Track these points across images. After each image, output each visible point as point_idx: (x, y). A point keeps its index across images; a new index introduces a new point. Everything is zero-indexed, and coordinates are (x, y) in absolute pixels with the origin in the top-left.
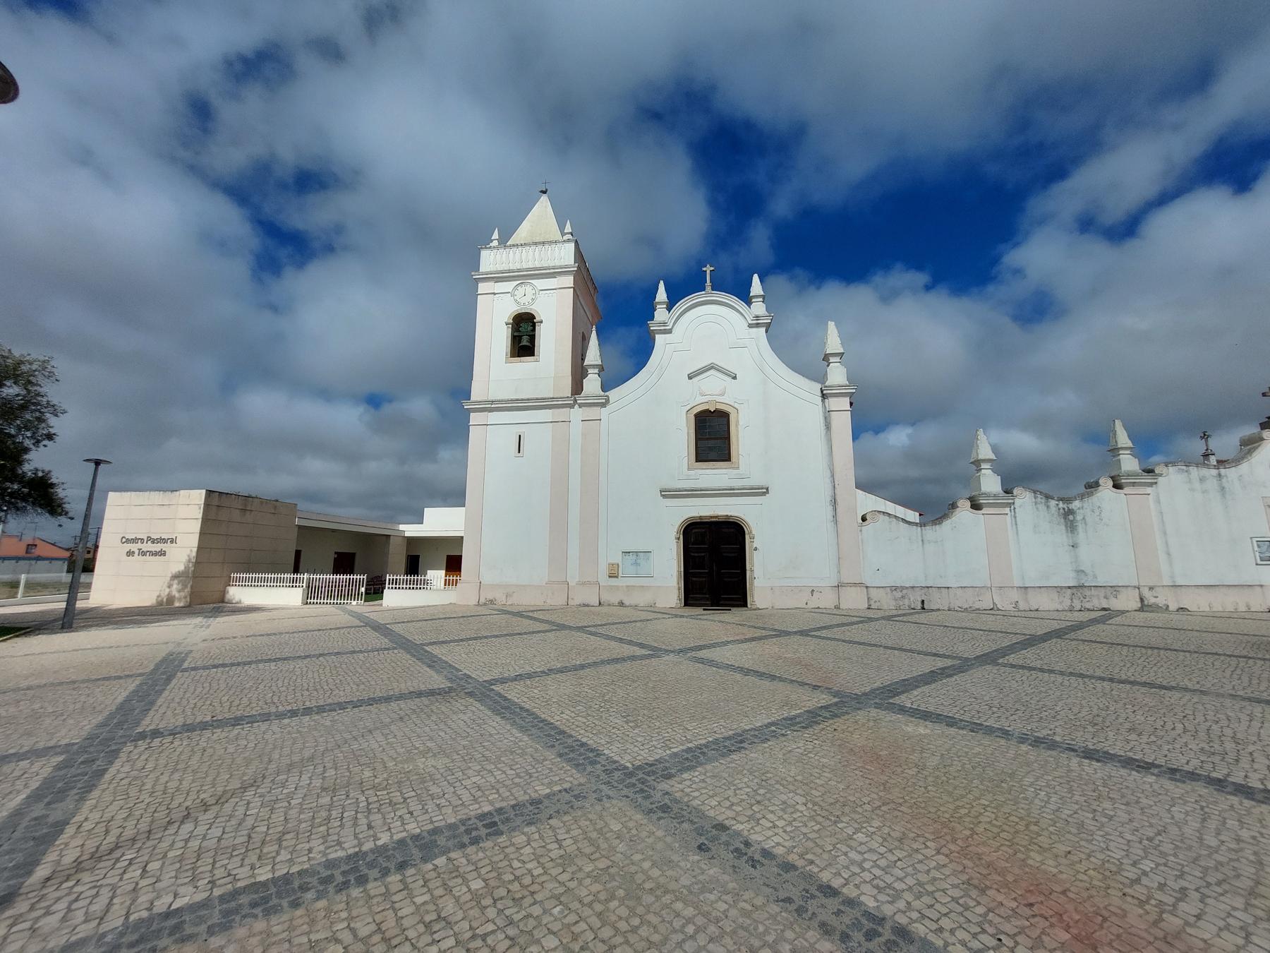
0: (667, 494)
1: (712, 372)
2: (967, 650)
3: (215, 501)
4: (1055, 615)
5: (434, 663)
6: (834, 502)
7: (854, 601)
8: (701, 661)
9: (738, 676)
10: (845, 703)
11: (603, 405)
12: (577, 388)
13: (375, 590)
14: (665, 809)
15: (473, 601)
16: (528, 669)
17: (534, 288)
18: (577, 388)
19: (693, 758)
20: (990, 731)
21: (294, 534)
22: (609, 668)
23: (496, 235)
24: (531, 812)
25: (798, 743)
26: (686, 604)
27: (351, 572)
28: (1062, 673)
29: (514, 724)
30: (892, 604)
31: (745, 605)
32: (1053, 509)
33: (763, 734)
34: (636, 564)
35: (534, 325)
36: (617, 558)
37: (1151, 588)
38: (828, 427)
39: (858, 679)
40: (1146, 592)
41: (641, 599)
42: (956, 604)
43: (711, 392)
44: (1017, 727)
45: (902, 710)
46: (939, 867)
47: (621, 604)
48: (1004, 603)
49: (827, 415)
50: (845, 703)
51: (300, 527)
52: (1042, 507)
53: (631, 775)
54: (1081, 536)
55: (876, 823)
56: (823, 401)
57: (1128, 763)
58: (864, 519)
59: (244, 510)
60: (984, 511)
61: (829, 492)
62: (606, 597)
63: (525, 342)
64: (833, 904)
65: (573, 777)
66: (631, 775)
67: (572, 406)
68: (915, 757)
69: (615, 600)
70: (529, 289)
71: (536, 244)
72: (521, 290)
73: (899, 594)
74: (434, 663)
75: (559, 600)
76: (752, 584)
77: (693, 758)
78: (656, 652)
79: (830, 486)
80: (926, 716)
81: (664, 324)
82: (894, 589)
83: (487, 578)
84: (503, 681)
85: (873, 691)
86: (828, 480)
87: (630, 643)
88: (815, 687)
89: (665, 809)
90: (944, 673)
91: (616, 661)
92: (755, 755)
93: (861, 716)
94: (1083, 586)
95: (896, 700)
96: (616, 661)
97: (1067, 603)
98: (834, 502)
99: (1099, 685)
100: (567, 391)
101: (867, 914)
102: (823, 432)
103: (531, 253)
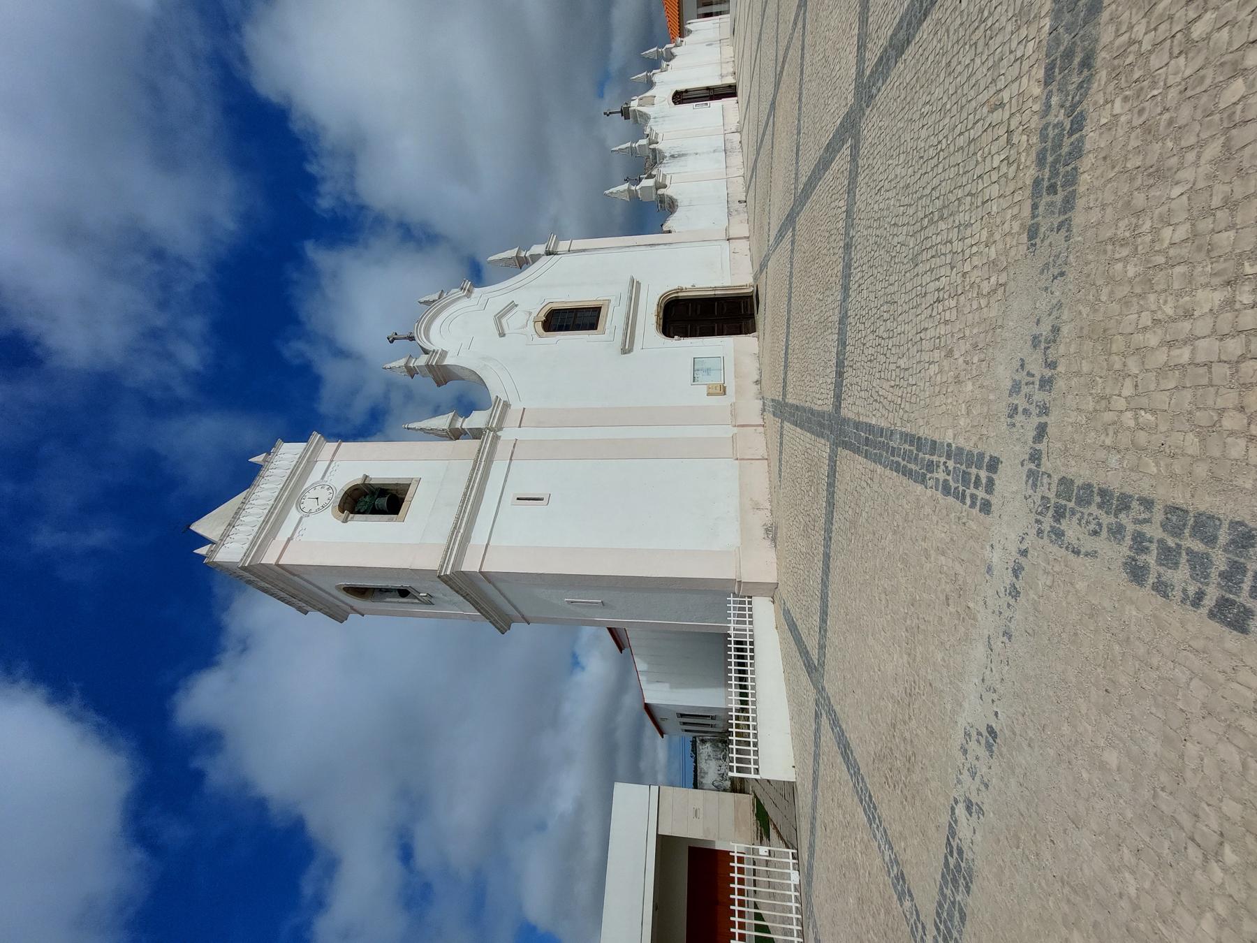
0: (626, 350)
1: (504, 321)
11: (507, 405)
17: (314, 486)
23: (202, 551)
36: (704, 389)
60: (667, 183)
63: (382, 502)
67: (498, 438)
72: (308, 504)
82: (729, 214)
83: (729, 537)
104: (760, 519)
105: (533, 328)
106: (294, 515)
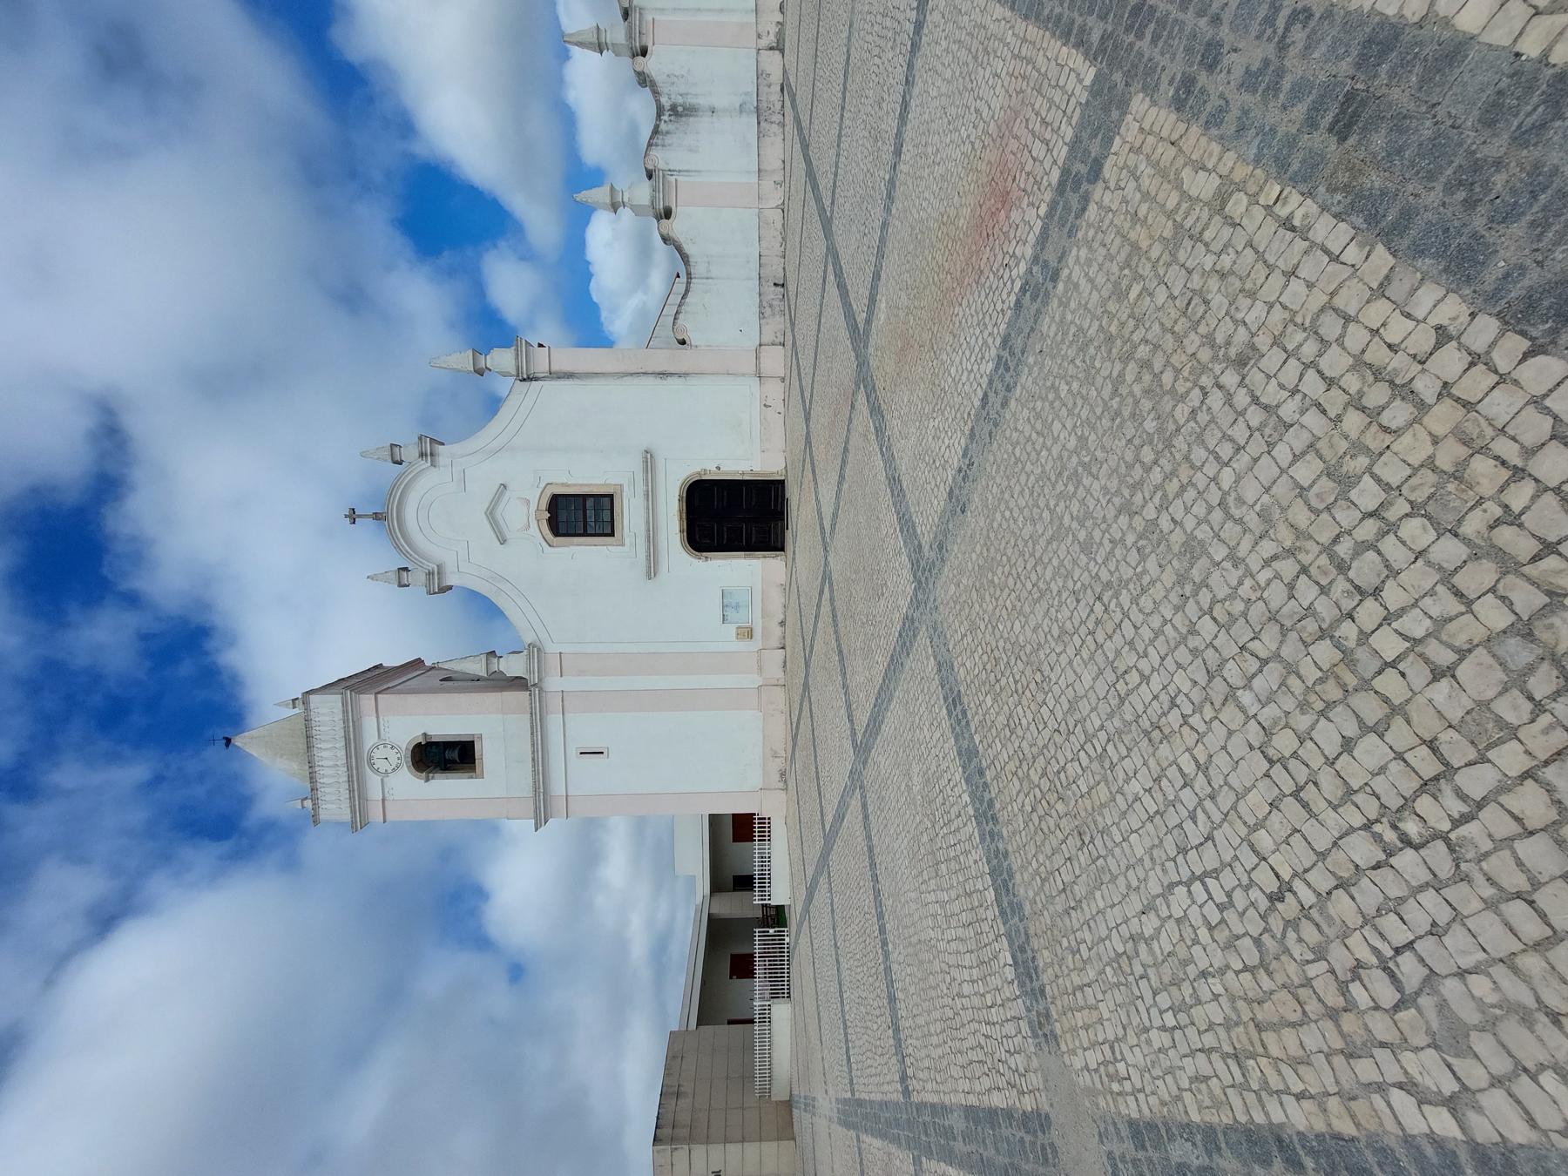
0: (652, 571)
1: (498, 514)
2: (820, 248)
3: (667, 1131)
4: (789, 142)
5: (840, 818)
6: (663, 375)
7: (775, 361)
8: (833, 526)
9: (845, 486)
10: (863, 378)
12: (518, 683)
13: (776, 916)
14: (940, 547)
15: (783, 795)
16: (843, 711)
18: (518, 683)
19: (906, 525)
20: (882, 240)
21: (708, 1030)
22: (841, 624)
24: (944, 667)
25: (894, 425)
26: (782, 549)
27: (752, 956)
28: (838, 155)
29: (886, 709)
30: (779, 319)
31: (782, 482)
32: (671, 127)
33: (889, 460)
34: (737, 606)
35: (430, 745)
36: (731, 629)
37: (759, 36)
38: (570, 375)
39: (842, 366)
40: (764, 42)
41: (777, 600)
42: (778, 250)
43: (525, 515)
44: (878, 213)
45: (868, 321)
46: (969, 306)
47: (782, 623)
48: (776, 198)
49: (554, 375)
50: (863, 378)
51: (698, 1024)
52: (668, 140)
53: (920, 582)
54: (701, 101)
55: (944, 357)
56: (536, 379)
57: (903, 118)
58: (683, 342)
59: (678, 1095)
61: (651, 380)
62: (775, 642)
63: (455, 755)
64: (992, 397)
65: (923, 639)
66: (920, 582)
68: (902, 314)
69: (778, 631)
70: (377, 754)
71: (309, 747)
72: (381, 765)
73: (768, 311)
74: (840, 818)
75: (779, 696)
76: (758, 474)
77: (906, 525)
78: (827, 577)
79: (644, 378)
80: (873, 300)
81: (430, 574)
82: (762, 315)
83: (755, 780)
84: (854, 733)
85: (854, 350)
86: (636, 380)
87: (819, 606)
88: (853, 406)
89: (940, 547)
90: (839, 274)
91: (834, 616)
92: (903, 465)
93: (873, 363)
94: (757, 108)
95: (861, 326)
96: (834, 616)
97: (775, 128)
98: (663, 375)
99: (847, 122)
100: (522, 696)
101: (996, 368)
102: (577, 382)
103: (324, 754)
104: (776, 765)
105: (537, 530)
106: (373, 783)
